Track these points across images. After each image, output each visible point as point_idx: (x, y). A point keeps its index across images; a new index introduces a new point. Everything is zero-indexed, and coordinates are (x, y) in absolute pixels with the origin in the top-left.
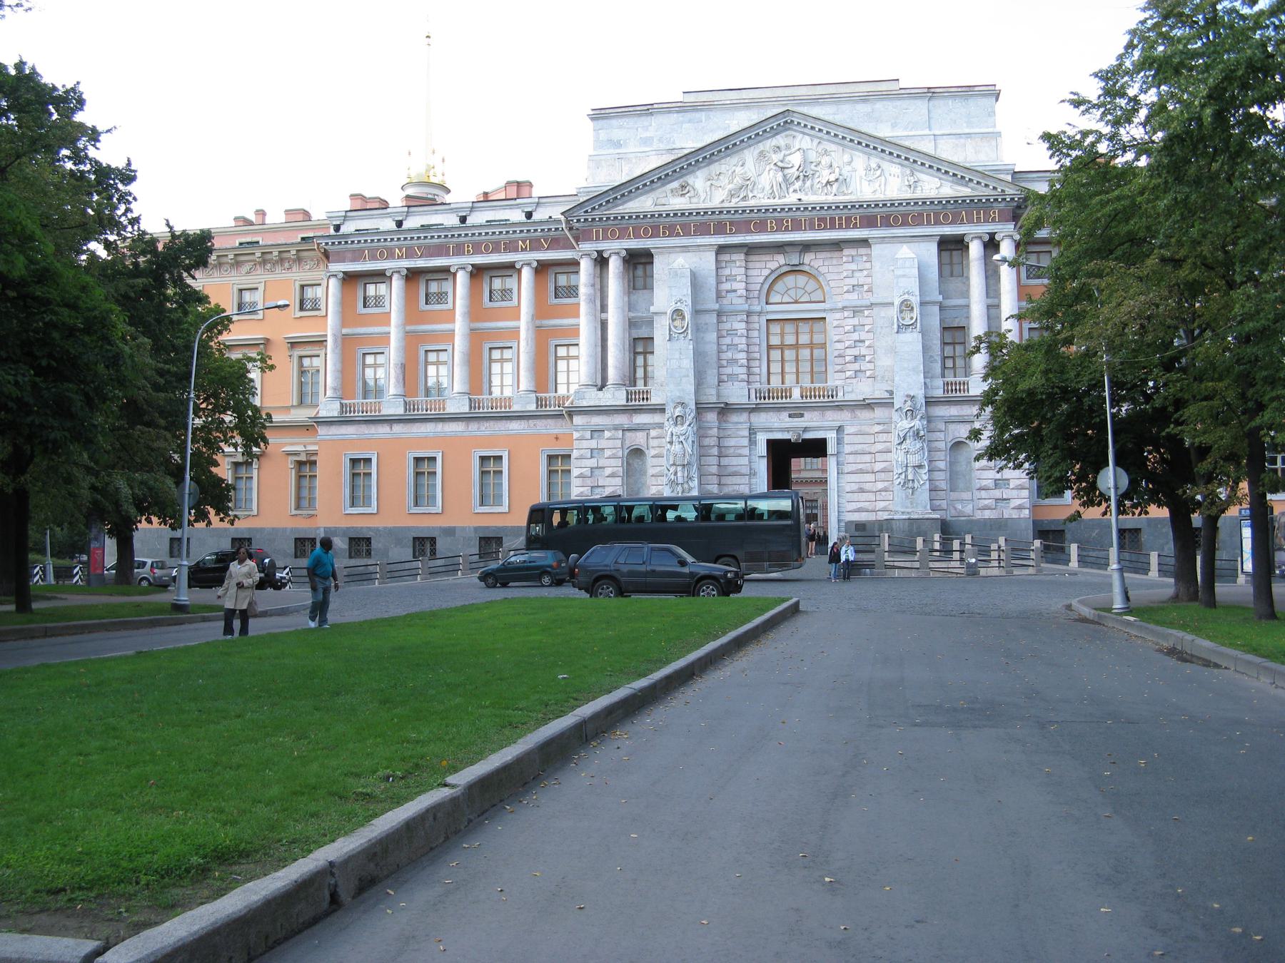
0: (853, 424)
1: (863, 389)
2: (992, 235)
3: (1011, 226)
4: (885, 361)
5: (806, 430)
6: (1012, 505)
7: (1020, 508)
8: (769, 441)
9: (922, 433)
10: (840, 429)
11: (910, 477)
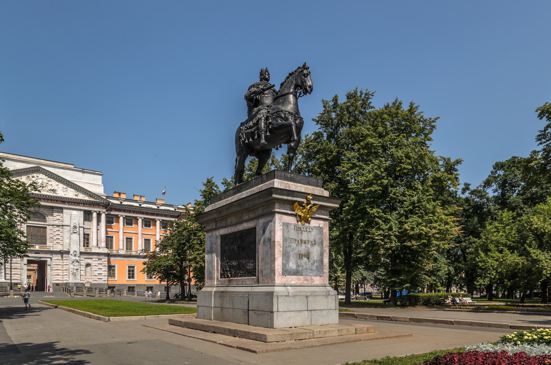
0: (56, 257)
1: (59, 248)
2: (100, 212)
3: (104, 210)
4: (67, 241)
5: (40, 258)
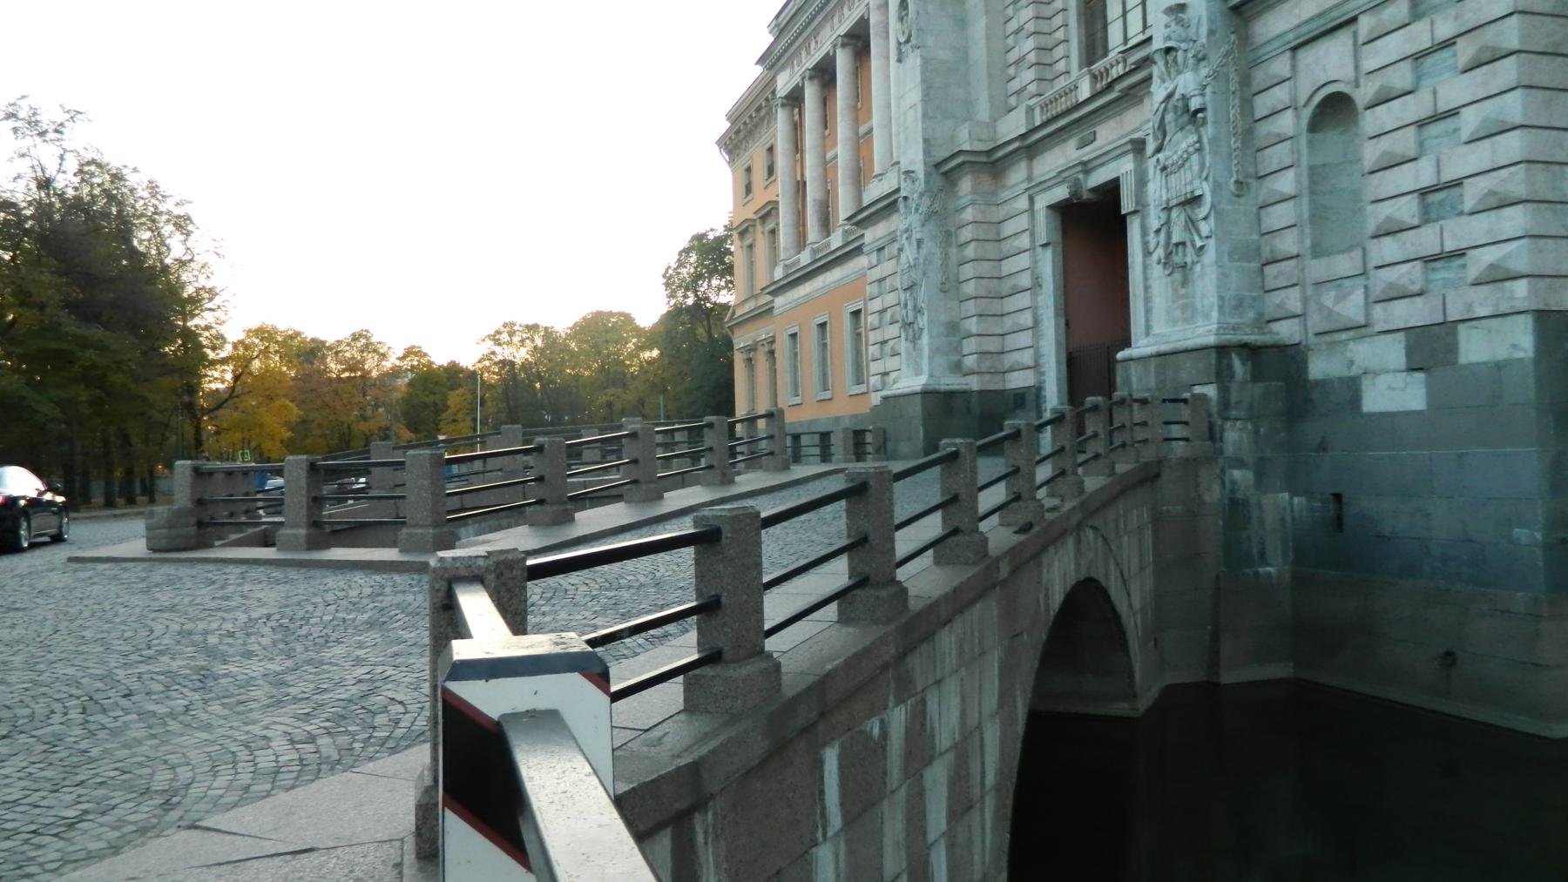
5: (1086, 167)
6: (1472, 273)
7: (1497, 277)
8: (1051, 207)
9: (1195, 103)
10: (1138, 146)
11: (1175, 239)
